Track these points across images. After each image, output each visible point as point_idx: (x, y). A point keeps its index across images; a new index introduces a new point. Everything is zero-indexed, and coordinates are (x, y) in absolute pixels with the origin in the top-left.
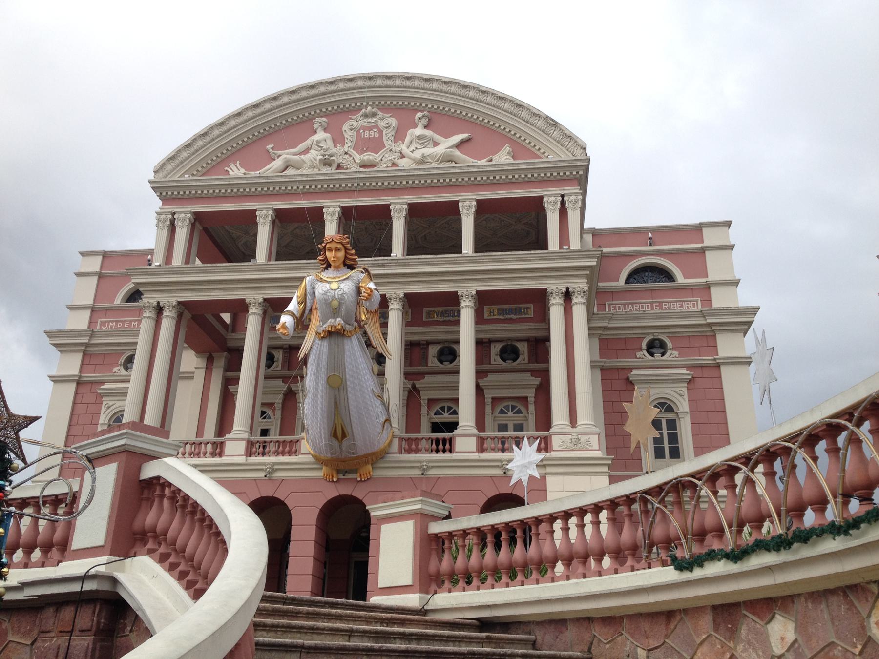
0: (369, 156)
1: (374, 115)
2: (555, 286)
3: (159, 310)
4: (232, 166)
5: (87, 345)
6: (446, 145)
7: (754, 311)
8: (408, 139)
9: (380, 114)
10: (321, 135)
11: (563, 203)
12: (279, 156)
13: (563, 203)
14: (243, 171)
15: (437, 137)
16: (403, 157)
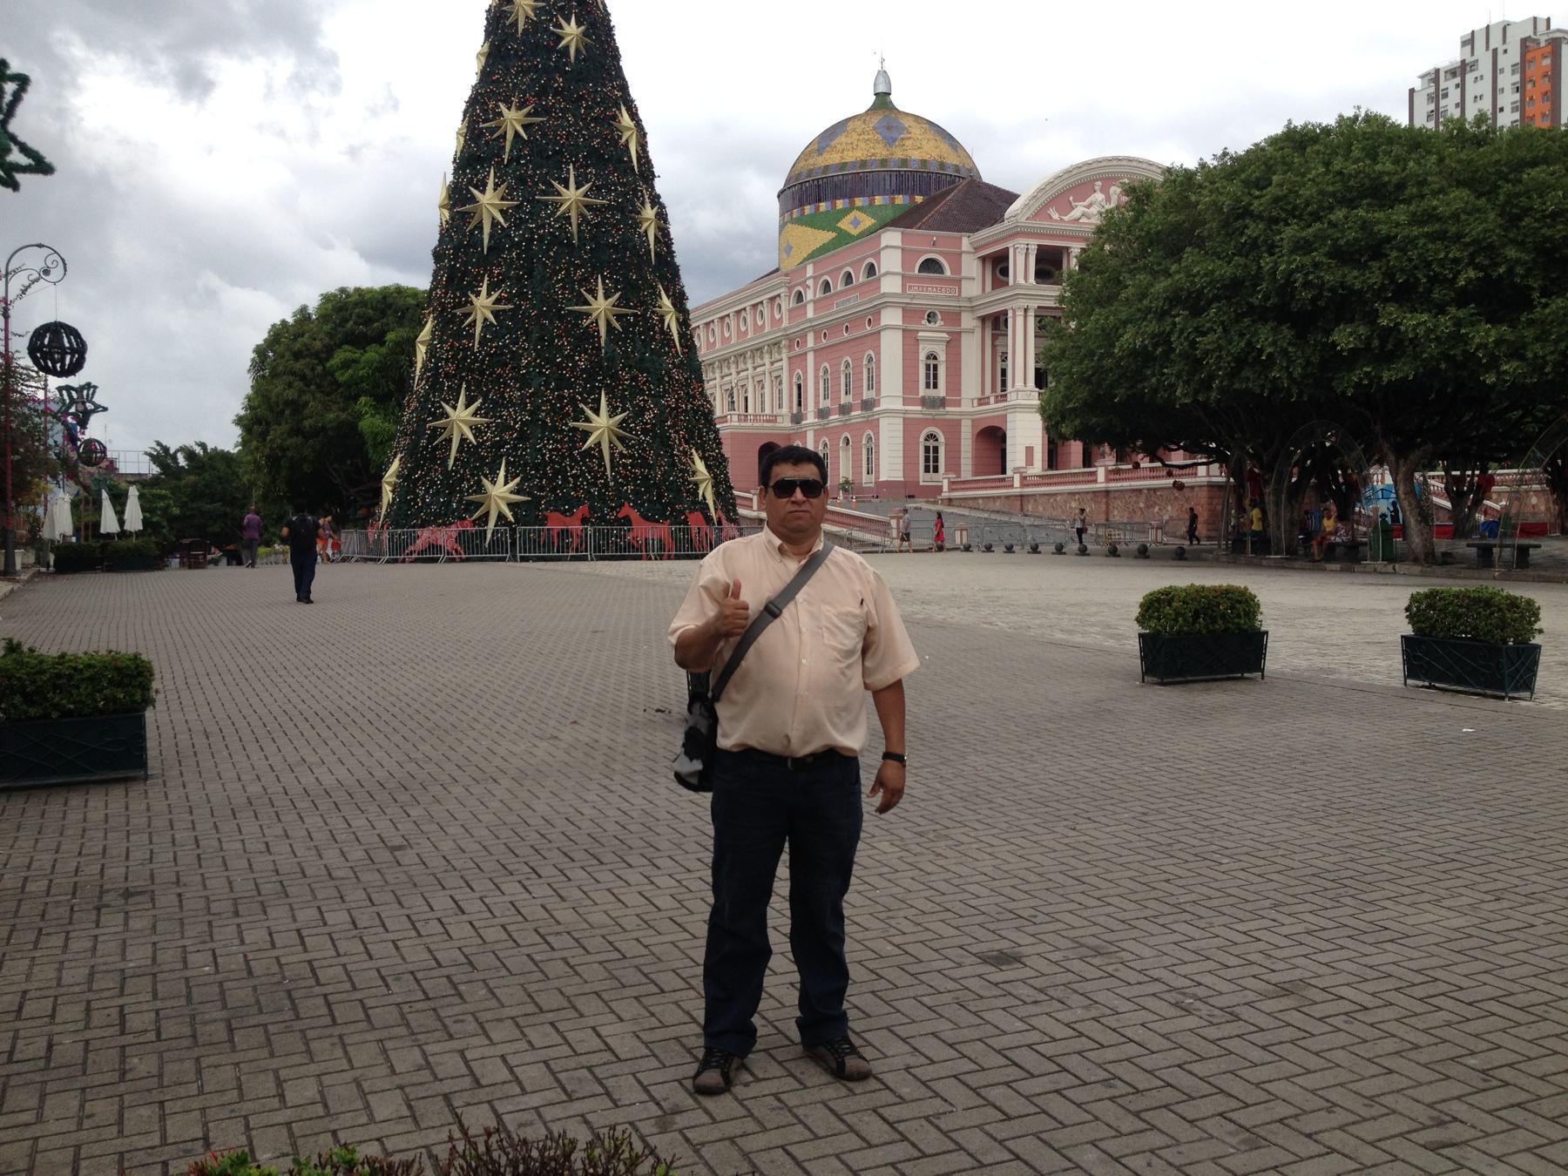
3: (1026, 310)
14: (1056, 216)
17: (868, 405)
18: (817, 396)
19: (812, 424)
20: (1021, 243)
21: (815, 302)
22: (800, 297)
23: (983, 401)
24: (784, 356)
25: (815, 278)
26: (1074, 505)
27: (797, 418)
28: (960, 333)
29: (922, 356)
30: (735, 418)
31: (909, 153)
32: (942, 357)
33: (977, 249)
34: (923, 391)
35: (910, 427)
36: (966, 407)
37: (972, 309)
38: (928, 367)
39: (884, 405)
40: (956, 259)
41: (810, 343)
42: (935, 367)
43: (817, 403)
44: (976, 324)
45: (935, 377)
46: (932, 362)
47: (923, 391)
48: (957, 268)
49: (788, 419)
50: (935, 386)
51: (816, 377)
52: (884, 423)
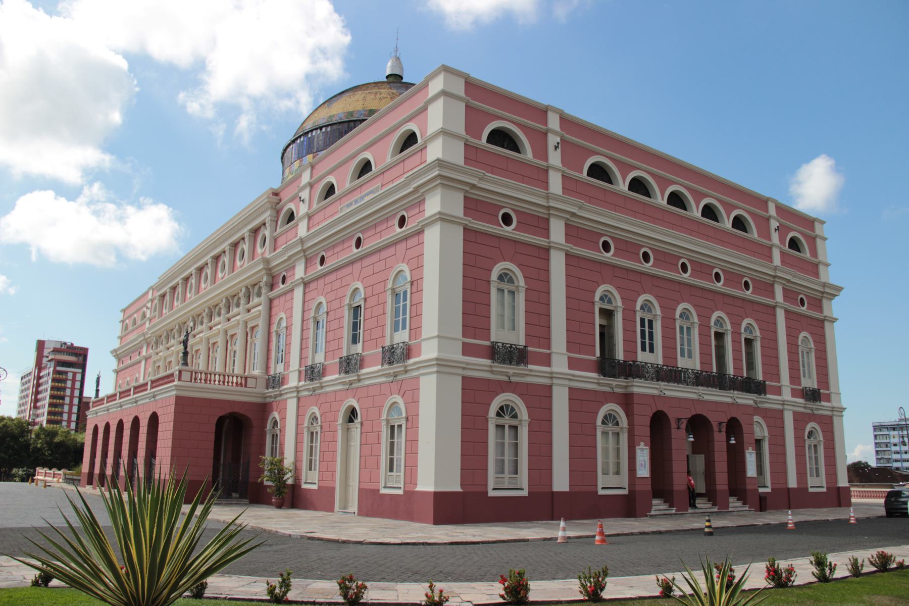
17: (391, 355)
19: (298, 390)
21: (310, 217)
22: (291, 217)
24: (263, 299)
25: (311, 185)
27: (275, 382)
28: (547, 250)
30: (186, 376)
35: (475, 395)
39: (429, 351)
40: (540, 138)
41: (299, 272)
46: (506, 286)
48: (542, 152)
52: (429, 387)
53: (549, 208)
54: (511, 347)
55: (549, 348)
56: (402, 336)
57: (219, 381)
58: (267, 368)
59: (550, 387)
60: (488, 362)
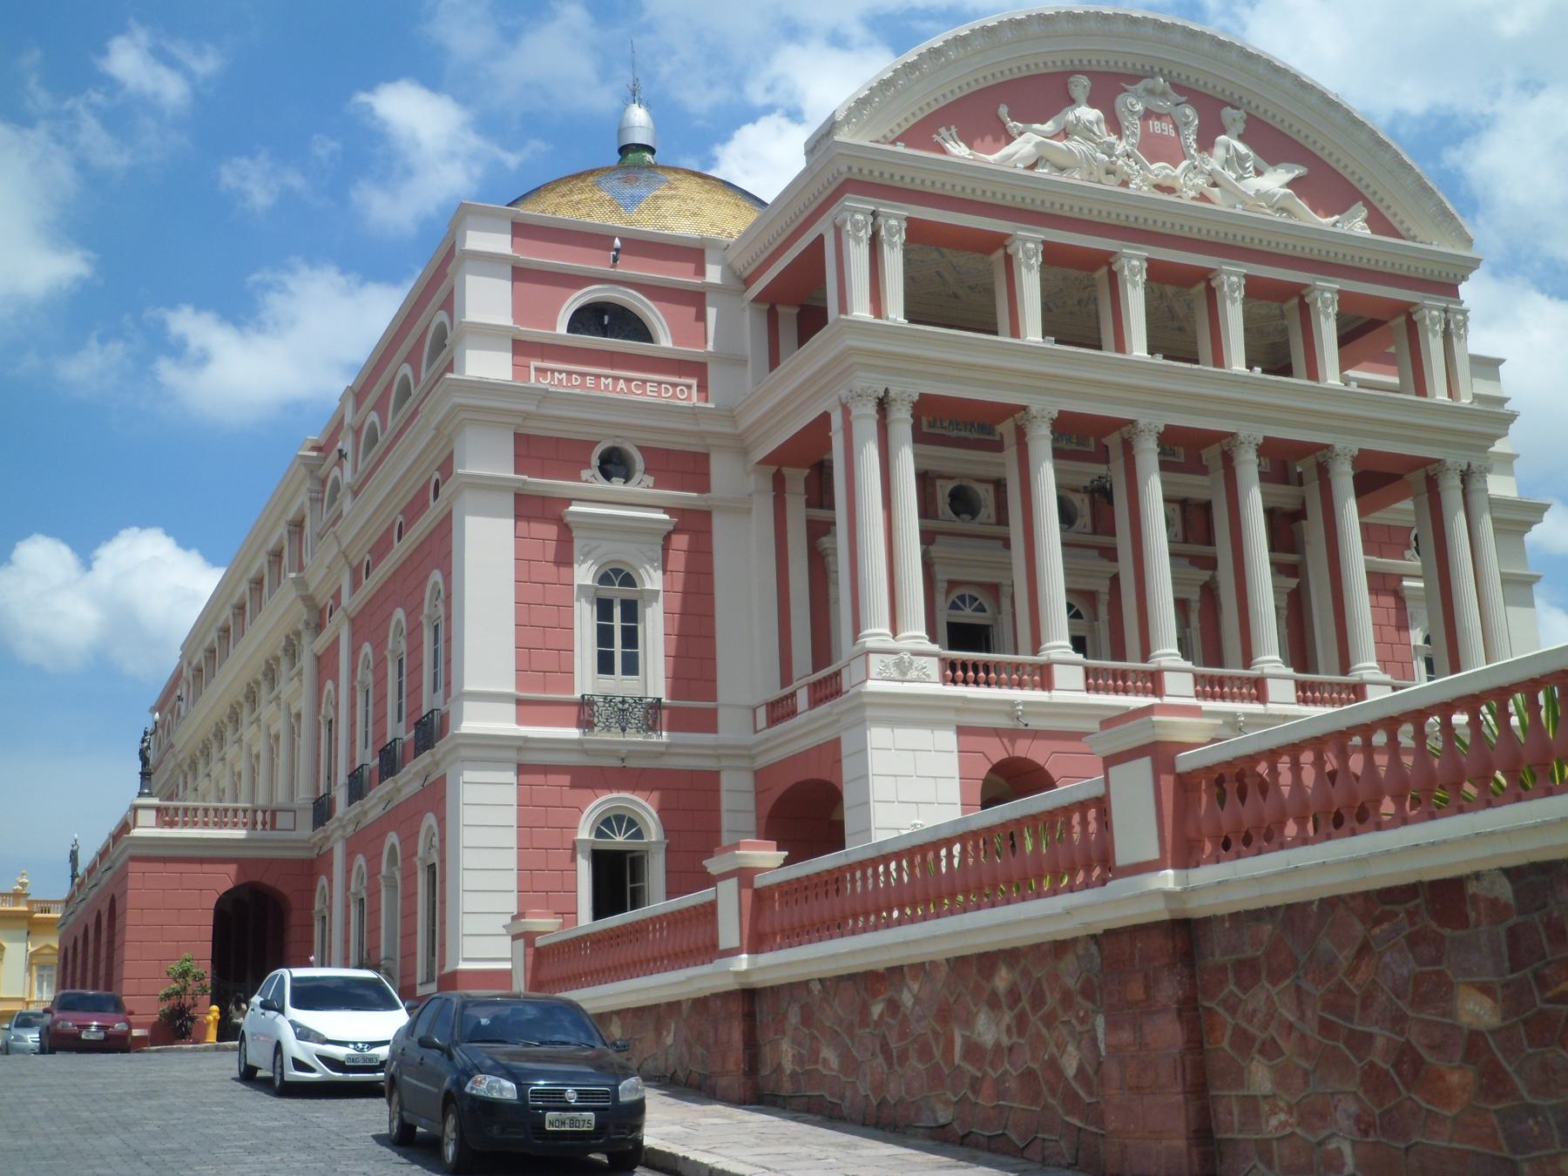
0: (1160, 169)
1: (1163, 95)
2: (1455, 459)
3: (883, 405)
4: (943, 130)
5: (527, 416)
6: (1275, 181)
7: (1543, 508)
8: (1219, 152)
9: (1174, 96)
10: (1087, 113)
11: (1447, 324)
12: (1021, 134)
13: (1447, 324)
15: (1262, 163)
16: (1215, 185)
18: (353, 742)
20: (856, 210)
23: (780, 710)
26: (988, 1030)
27: (322, 811)
28: (705, 515)
29: (584, 574)
31: (670, 222)
32: (652, 580)
33: (748, 282)
34: (586, 680)
36: (734, 728)
37: (740, 446)
38: (604, 609)
42: (631, 611)
43: (353, 760)
44: (757, 487)
45: (630, 638)
46: (616, 592)
47: (586, 680)
49: (307, 818)
50: (631, 667)
51: (353, 689)
53: (702, 435)
54: (623, 702)
55: (713, 697)
56: (438, 701)
57: (264, 824)
58: (318, 789)
59: (714, 776)
60: (573, 733)
